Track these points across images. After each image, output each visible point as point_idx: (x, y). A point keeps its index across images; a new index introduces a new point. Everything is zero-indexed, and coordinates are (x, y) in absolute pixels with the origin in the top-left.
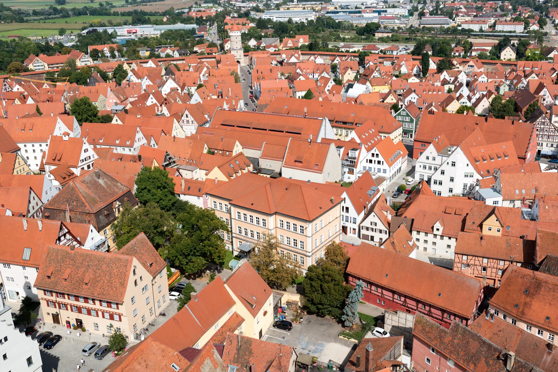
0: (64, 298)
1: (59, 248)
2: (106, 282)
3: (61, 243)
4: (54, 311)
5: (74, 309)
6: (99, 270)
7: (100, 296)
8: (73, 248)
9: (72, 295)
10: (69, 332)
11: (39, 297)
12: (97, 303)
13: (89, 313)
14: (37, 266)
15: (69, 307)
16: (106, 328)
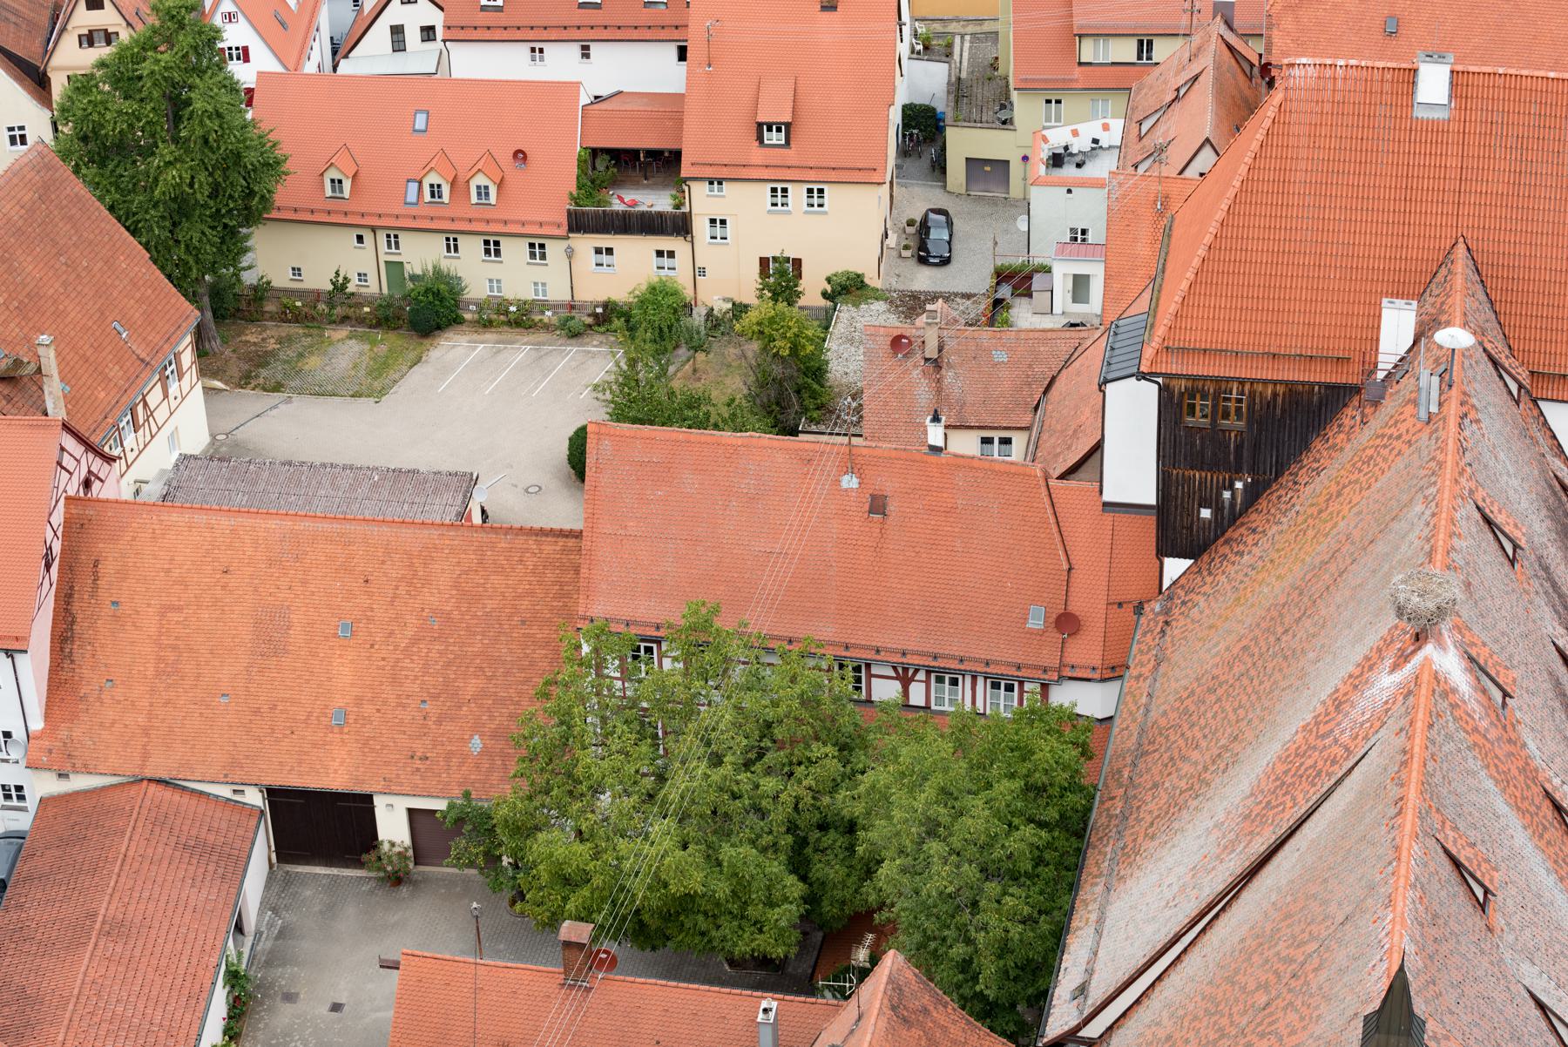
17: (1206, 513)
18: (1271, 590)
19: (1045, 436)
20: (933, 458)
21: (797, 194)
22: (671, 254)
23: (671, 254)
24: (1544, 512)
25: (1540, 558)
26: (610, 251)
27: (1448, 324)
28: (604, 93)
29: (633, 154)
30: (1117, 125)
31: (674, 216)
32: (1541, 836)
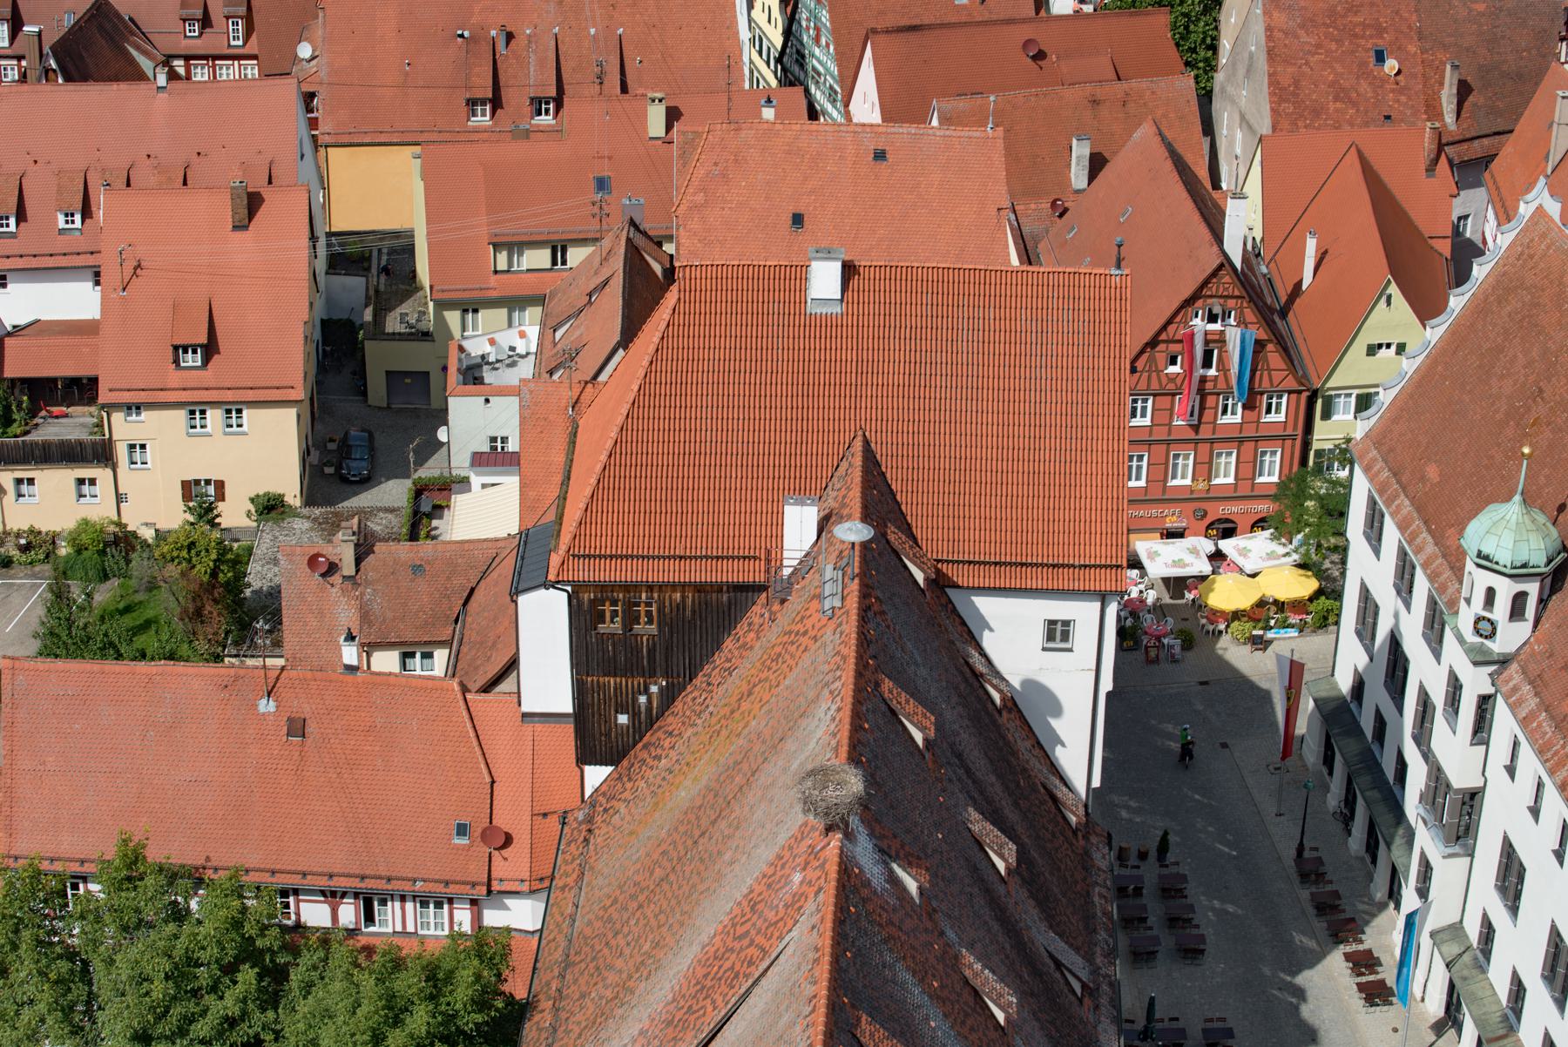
17: (623, 719)
18: (685, 793)
19: (464, 649)
20: (350, 678)
21: (214, 417)
22: (93, 482)
23: (93, 482)
24: (955, 699)
25: (952, 746)
26: (31, 481)
27: (849, 517)
28: (22, 321)
29: (54, 380)
30: (533, 332)
31: (94, 443)
32: (963, 1023)
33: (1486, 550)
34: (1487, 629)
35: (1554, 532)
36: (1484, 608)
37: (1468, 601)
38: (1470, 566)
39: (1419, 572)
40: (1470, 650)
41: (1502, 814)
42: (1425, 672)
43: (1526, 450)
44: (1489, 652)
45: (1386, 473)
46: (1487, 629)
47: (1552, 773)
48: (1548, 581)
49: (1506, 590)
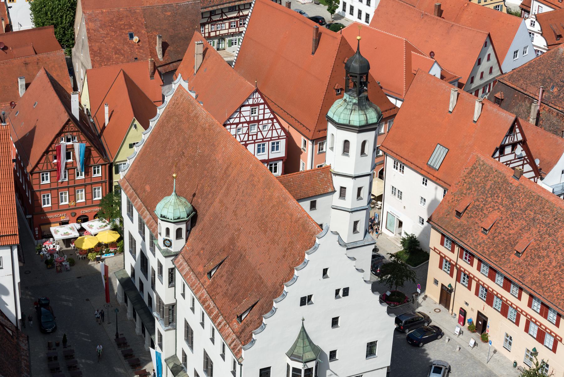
0: (472, 264)
1: (495, 166)
2: (554, 264)
3: (503, 159)
4: (447, 280)
5: (480, 293)
6: (550, 236)
7: (534, 287)
8: (519, 174)
9: (486, 264)
10: (458, 330)
11: (431, 245)
12: (525, 297)
13: (504, 311)
14: (447, 186)
15: (474, 284)
16: (524, 352)
33: (164, 214)
34: (168, 243)
35: (189, 205)
36: (166, 236)
37: (160, 234)
38: (159, 221)
39: (145, 226)
40: (163, 252)
41: (183, 313)
42: (153, 263)
43: (174, 175)
44: (170, 252)
45: (132, 191)
46: (168, 243)
47: (195, 294)
48: (189, 223)
49: (173, 228)
